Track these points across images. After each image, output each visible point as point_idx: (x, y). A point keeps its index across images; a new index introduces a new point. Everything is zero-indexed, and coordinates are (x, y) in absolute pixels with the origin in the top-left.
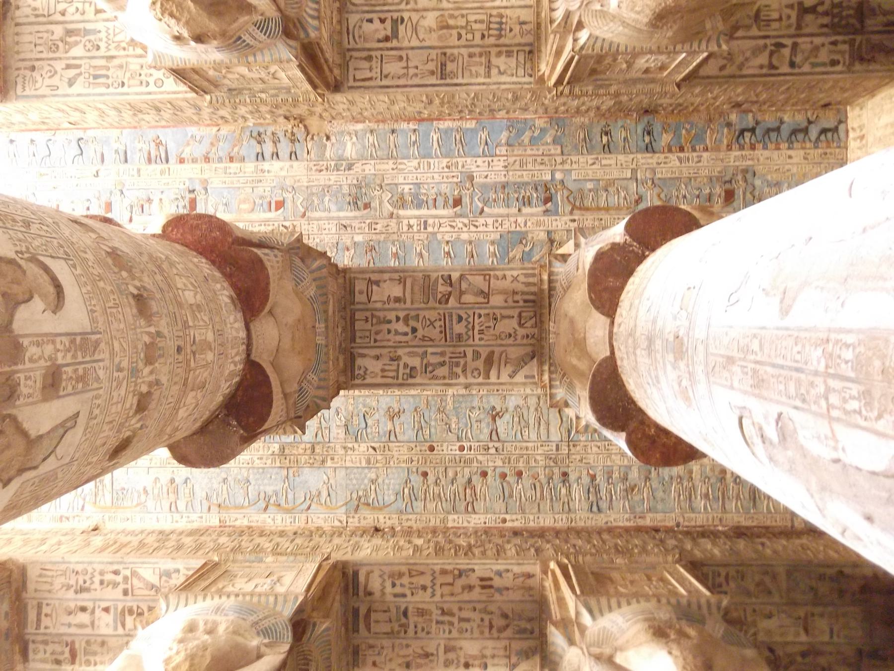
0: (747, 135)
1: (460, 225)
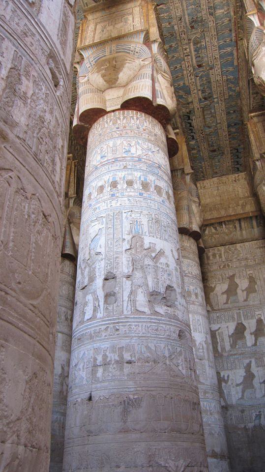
0: (236, 151)
1: (190, 70)
